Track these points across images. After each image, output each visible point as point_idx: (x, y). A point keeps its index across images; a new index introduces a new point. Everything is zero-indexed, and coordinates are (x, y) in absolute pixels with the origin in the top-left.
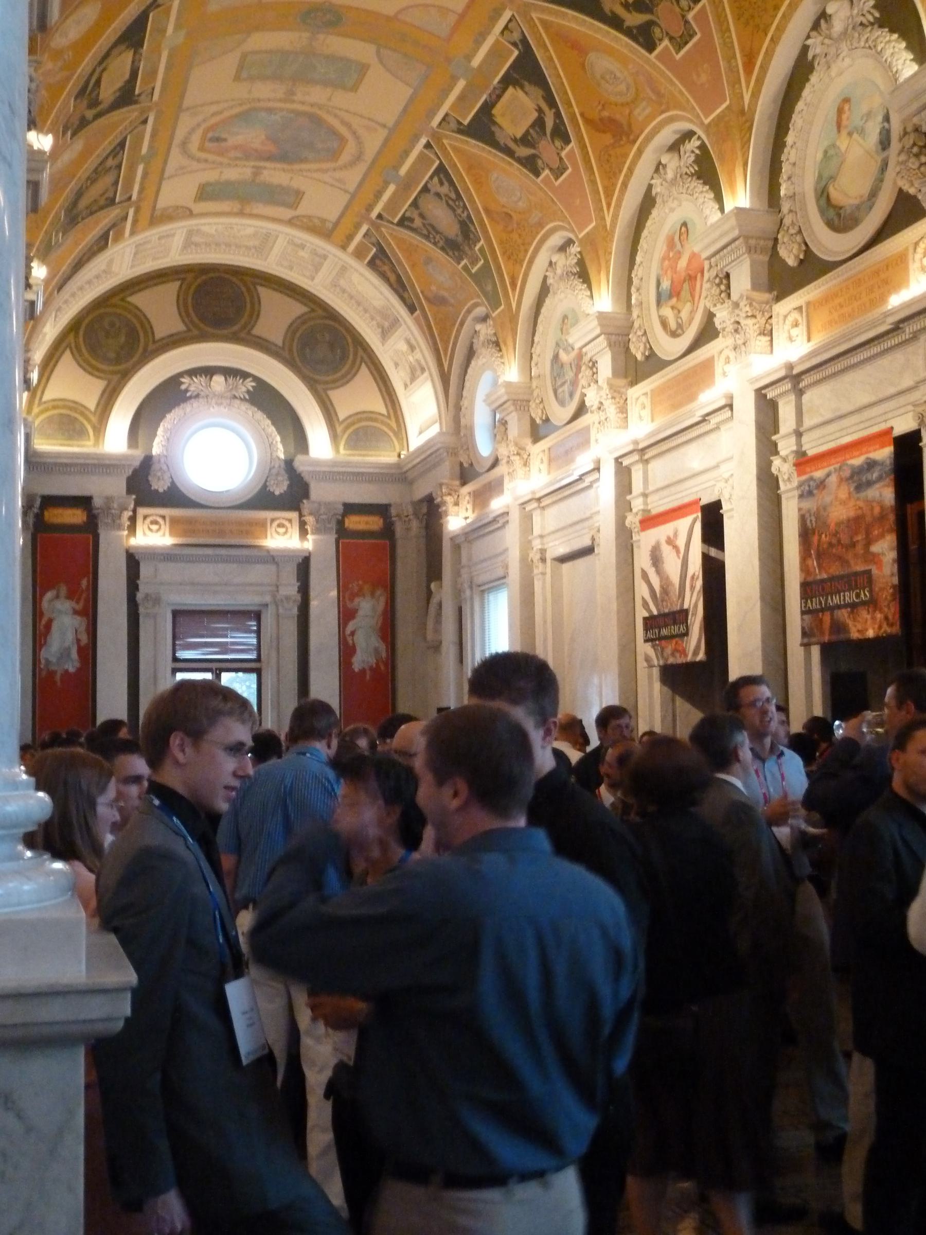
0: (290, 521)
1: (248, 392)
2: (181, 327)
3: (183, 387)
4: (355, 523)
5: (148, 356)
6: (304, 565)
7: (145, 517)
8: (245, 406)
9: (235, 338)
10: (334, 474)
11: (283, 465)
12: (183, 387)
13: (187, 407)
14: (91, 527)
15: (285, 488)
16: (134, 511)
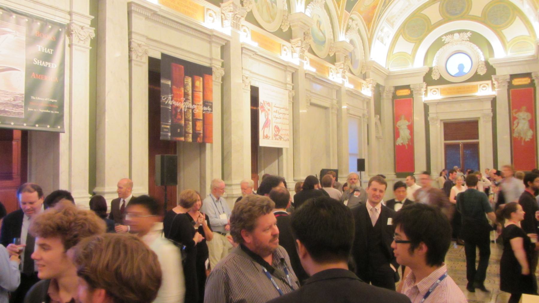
0: (488, 84)
1: (469, 37)
2: (441, 18)
3: (443, 40)
4: (517, 82)
5: (430, 31)
6: (494, 101)
7: (431, 90)
8: (468, 42)
9: (462, 18)
10: (505, 63)
11: (484, 63)
12: (443, 40)
13: (444, 47)
14: (411, 95)
15: (485, 72)
16: (426, 88)
